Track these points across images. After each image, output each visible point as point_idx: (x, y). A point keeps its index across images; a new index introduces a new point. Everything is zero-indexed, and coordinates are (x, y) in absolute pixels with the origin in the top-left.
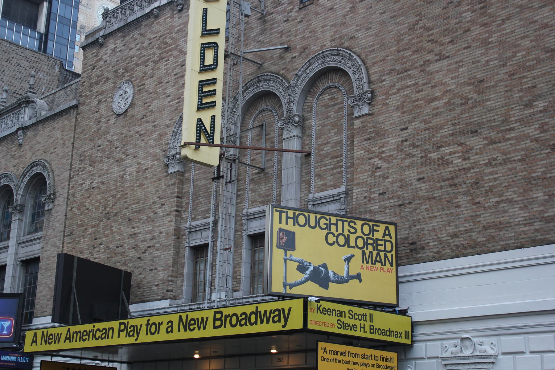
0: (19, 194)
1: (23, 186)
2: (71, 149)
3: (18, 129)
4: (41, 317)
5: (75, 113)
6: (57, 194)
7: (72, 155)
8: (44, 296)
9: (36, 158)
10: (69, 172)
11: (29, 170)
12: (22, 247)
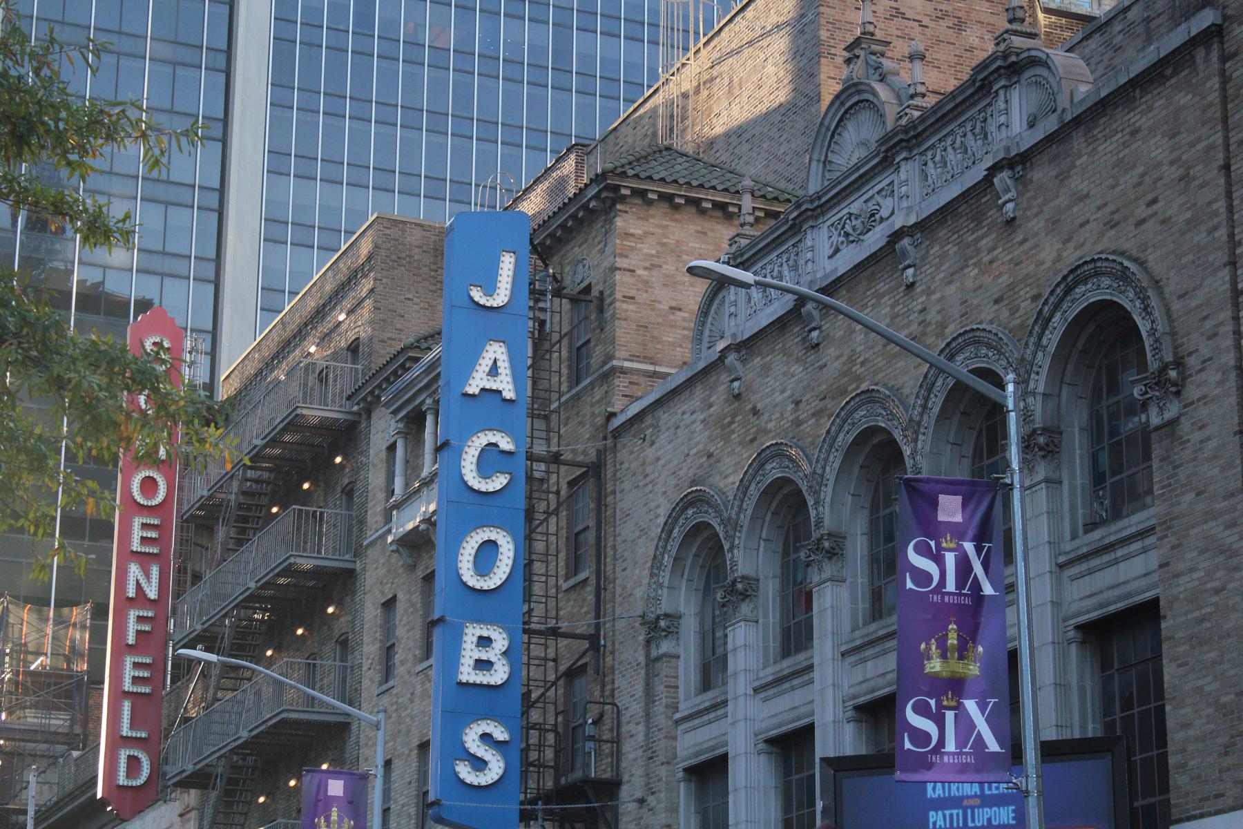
0: (1034, 394)
1: (1044, 361)
2: (1222, 190)
3: (994, 169)
4: (1202, 816)
5: (1215, 56)
6: (1192, 361)
7: (1230, 209)
8: (1198, 739)
9: (1078, 253)
10: (1225, 273)
11: (1061, 300)
12: (1074, 579)
